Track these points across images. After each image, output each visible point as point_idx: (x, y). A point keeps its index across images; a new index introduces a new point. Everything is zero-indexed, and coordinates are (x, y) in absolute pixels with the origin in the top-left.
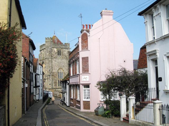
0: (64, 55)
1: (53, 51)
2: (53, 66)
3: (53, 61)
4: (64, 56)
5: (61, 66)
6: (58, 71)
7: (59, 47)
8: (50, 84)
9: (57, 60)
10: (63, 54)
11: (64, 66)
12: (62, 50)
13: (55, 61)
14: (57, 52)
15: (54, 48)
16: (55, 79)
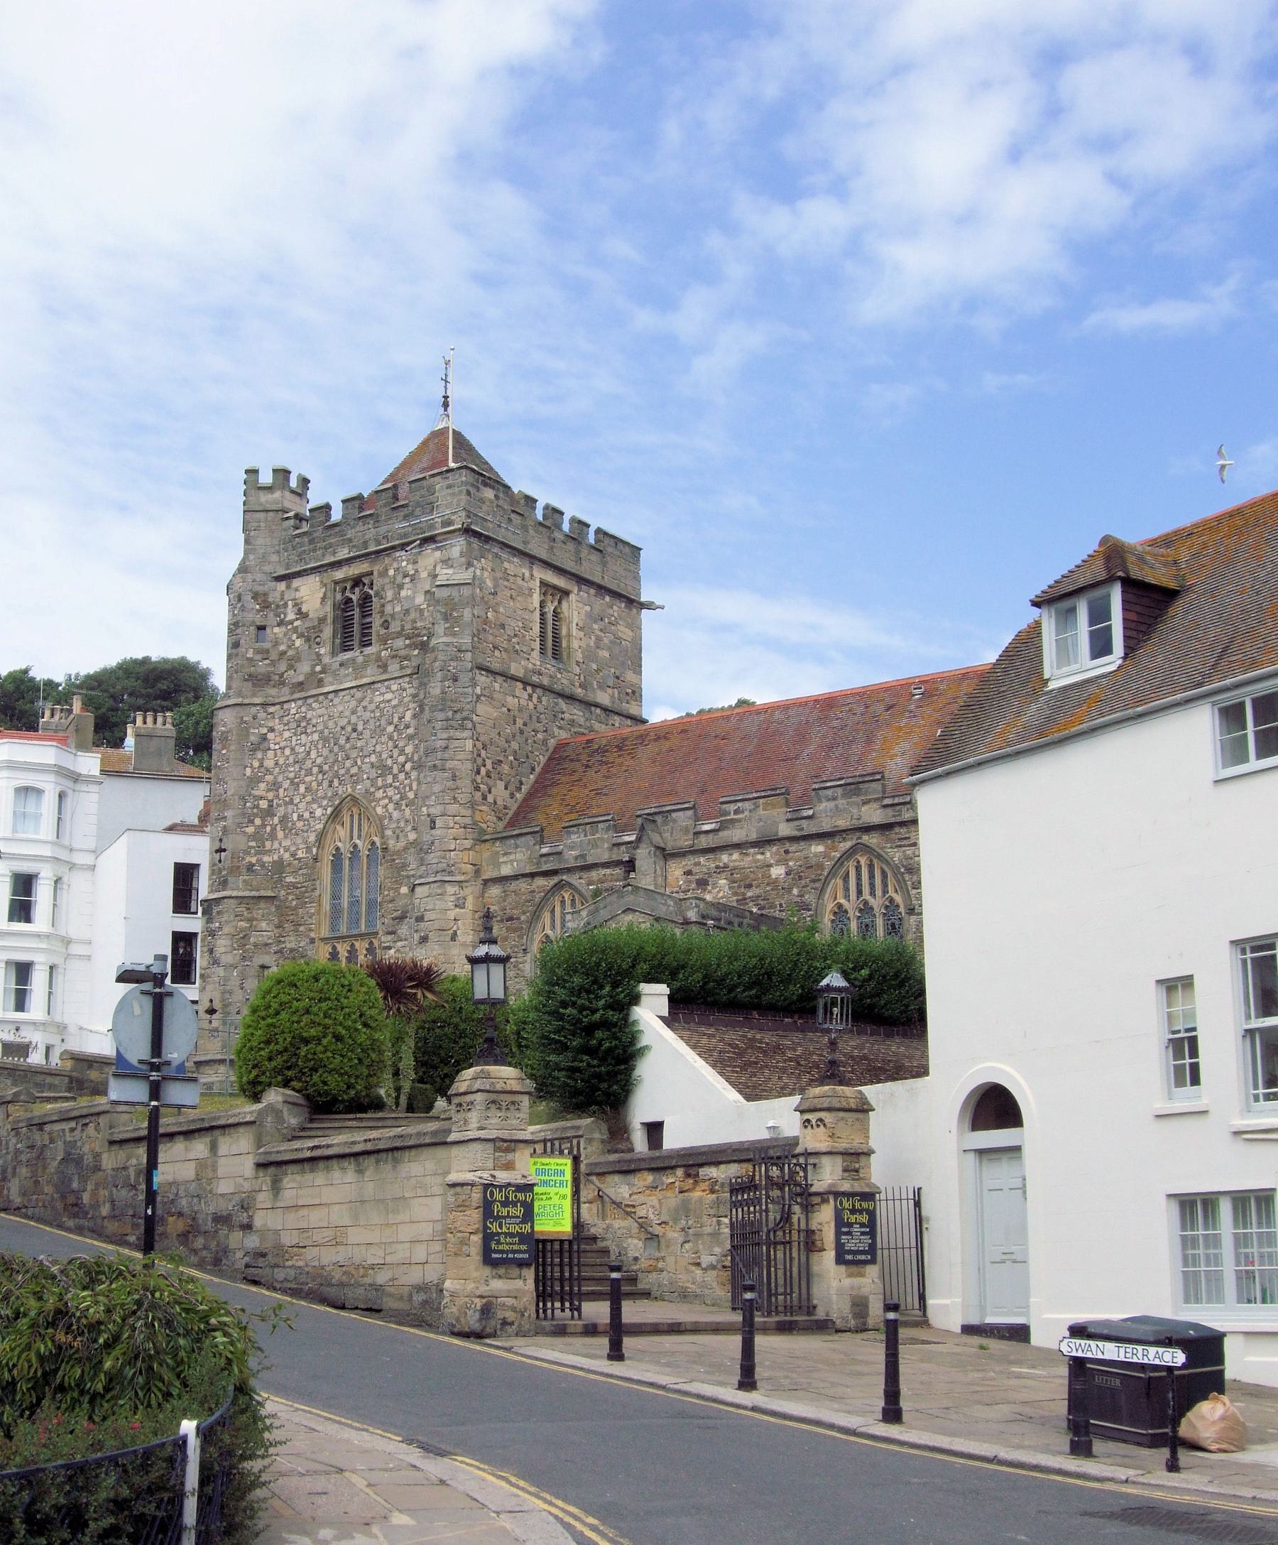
0: (399, 634)
1: (291, 616)
2: (275, 786)
3: (281, 737)
4: (400, 643)
5: (357, 783)
6: (321, 836)
7: (343, 553)
8: (211, 1011)
9: (316, 712)
10: (386, 625)
11: (384, 770)
12: (377, 568)
13: (302, 726)
14: (322, 620)
15: (296, 583)
16: (291, 942)
